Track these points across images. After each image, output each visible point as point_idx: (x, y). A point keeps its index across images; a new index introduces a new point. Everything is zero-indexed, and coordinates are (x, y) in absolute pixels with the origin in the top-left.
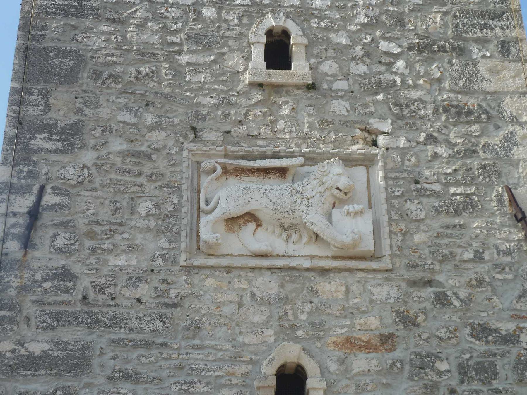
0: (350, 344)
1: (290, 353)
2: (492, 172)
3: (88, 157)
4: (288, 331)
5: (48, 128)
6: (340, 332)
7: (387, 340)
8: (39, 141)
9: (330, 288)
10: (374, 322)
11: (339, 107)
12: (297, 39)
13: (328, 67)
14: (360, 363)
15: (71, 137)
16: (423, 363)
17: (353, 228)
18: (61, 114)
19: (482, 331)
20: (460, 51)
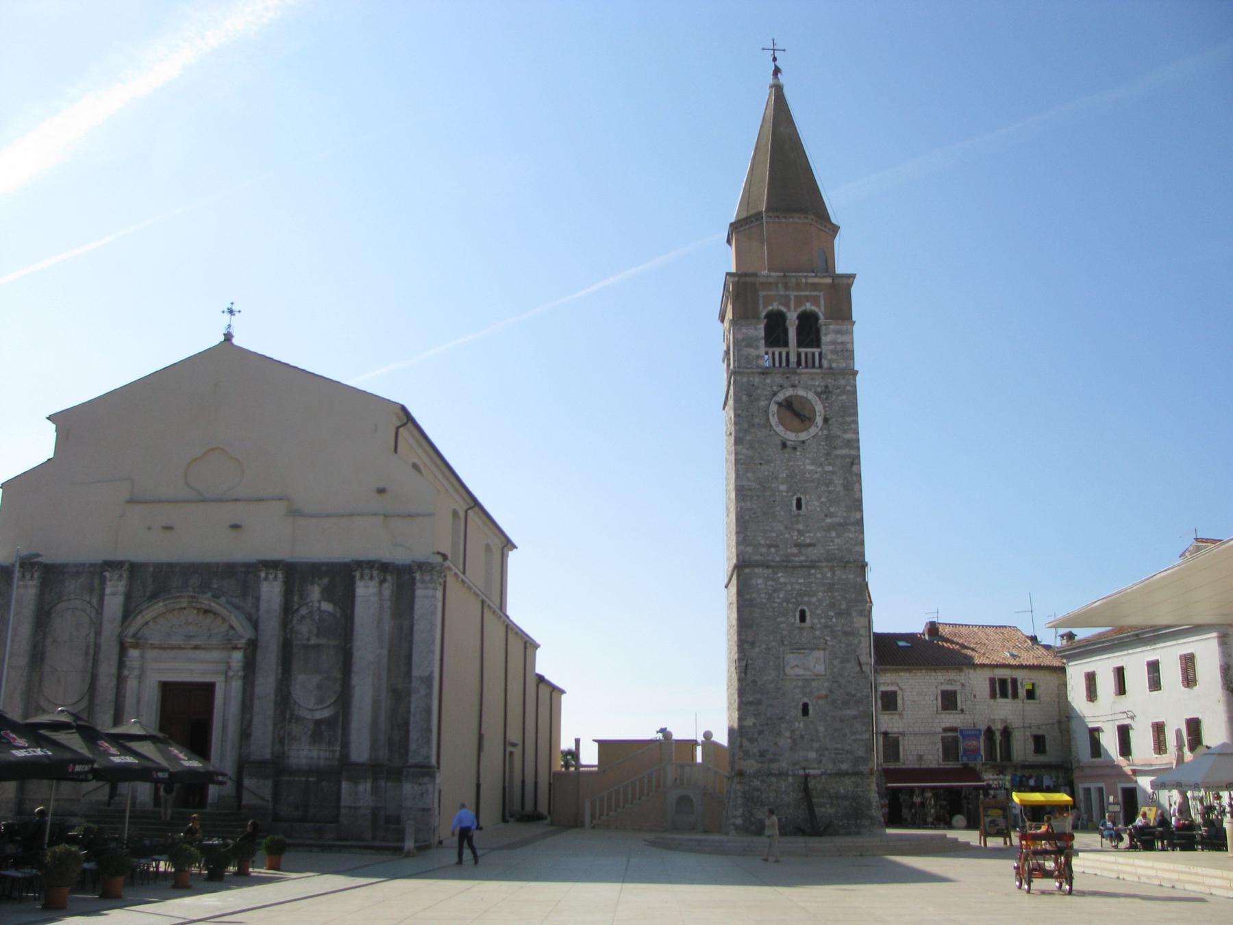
0: (819, 698)
1: (806, 700)
2: (855, 651)
3: (757, 650)
4: (805, 695)
5: (747, 642)
6: (816, 694)
7: (826, 696)
8: (746, 646)
9: (814, 684)
10: (824, 692)
11: (818, 633)
12: (808, 614)
13: (816, 621)
14: (820, 702)
15: (753, 644)
16: (834, 701)
17: (820, 668)
18: (750, 638)
19: (848, 694)
20: (850, 614)
